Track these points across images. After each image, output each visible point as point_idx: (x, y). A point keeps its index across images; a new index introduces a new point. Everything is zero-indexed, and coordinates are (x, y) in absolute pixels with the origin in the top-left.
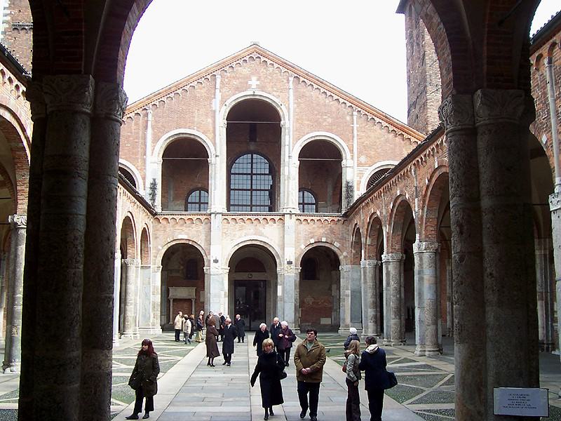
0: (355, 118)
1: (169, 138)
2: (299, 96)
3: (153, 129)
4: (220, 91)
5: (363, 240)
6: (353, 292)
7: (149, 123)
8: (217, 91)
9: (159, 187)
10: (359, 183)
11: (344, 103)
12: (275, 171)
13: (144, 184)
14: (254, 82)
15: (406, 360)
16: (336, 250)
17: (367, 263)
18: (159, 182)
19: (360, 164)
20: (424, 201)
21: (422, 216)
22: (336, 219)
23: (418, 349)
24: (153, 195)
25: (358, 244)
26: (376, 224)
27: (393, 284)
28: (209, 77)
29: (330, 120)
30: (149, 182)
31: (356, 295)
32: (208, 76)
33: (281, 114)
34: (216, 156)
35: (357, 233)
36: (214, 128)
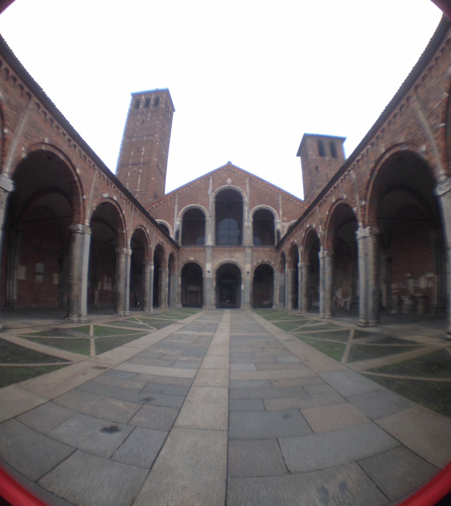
0: (280, 198)
1: (186, 208)
2: (251, 187)
3: (178, 204)
4: (212, 185)
5: (287, 258)
6: (280, 287)
7: (176, 202)
8: (211, 185)
9: (180, 234)
10: (283, 231)
11: (274, 191)
12: (240, 226)
13: (173, 231)
14: (229, 181)
15: (315, 321)
16: (272, 265)
17: (288, 270)
18: (181, 230)
19: (283, 221)
20: (326, 225)
21: (325, 235)
22: (272, 249)
23: (321, 315)
24: (177, 237)
25: (283, 262)
26: (294, 248)
27: (304, 279)
28: (206, 179)
29: (268, 199)
30: (175, 230)
31: (283, 289)
32: (206, 178)
33: (243, 195)
34: (210, 217)
35: (283, 256)
36: (208, 203)
